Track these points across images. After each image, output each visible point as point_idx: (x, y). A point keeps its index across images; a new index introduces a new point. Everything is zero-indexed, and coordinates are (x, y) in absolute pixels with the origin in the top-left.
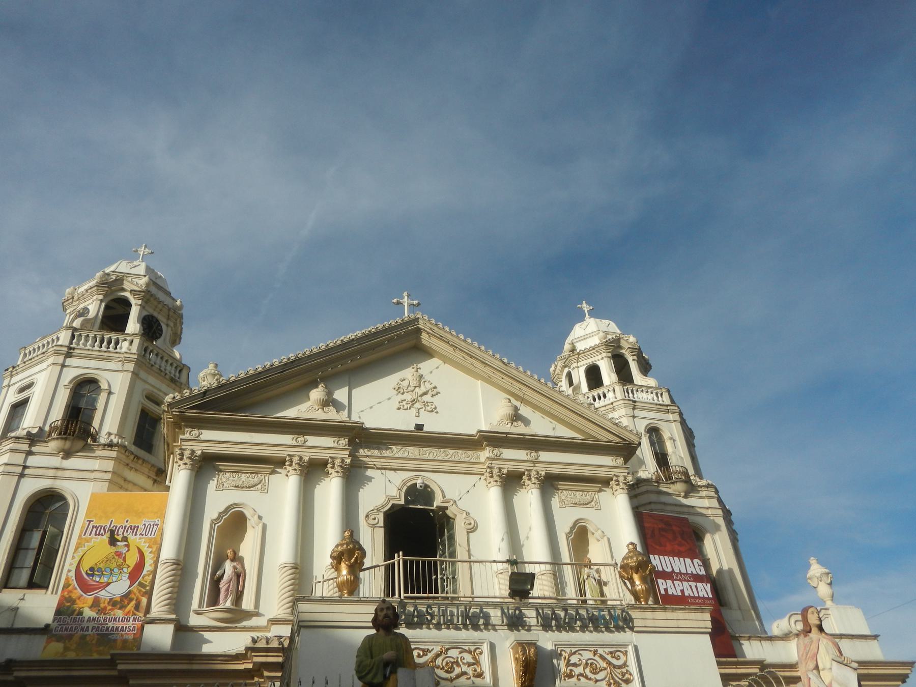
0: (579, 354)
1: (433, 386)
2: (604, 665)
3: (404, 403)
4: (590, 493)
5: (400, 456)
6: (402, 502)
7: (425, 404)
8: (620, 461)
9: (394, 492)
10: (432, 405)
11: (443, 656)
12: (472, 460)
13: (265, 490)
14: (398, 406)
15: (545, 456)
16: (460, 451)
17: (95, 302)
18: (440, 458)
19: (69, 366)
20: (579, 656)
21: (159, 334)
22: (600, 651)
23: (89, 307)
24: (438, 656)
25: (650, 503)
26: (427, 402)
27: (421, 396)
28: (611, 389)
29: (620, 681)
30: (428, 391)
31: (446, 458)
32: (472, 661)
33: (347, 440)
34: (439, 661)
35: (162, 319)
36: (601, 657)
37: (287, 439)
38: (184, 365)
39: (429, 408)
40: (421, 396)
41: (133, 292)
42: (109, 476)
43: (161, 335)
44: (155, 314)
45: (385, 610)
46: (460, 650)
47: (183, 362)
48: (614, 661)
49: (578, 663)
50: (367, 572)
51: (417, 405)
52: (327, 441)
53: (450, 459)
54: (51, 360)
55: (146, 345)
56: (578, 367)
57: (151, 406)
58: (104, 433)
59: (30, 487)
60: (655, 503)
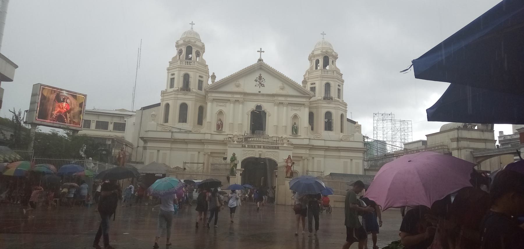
0: (314, 56)
7: (262, 84)
8: (308, 100)
9: (253, 108)
12: (272, 100)
13: (226, 107)
22: (273, 153)
34: (248, 153)
35: (199, 50)
38: (207, 65)
39: (262, 86)
42: (194, 100)
44: (198, 50)
48: (275, 154)
51: (260, 85)
57: (201, 79)
58: (191, 88)
59: (180, 102)
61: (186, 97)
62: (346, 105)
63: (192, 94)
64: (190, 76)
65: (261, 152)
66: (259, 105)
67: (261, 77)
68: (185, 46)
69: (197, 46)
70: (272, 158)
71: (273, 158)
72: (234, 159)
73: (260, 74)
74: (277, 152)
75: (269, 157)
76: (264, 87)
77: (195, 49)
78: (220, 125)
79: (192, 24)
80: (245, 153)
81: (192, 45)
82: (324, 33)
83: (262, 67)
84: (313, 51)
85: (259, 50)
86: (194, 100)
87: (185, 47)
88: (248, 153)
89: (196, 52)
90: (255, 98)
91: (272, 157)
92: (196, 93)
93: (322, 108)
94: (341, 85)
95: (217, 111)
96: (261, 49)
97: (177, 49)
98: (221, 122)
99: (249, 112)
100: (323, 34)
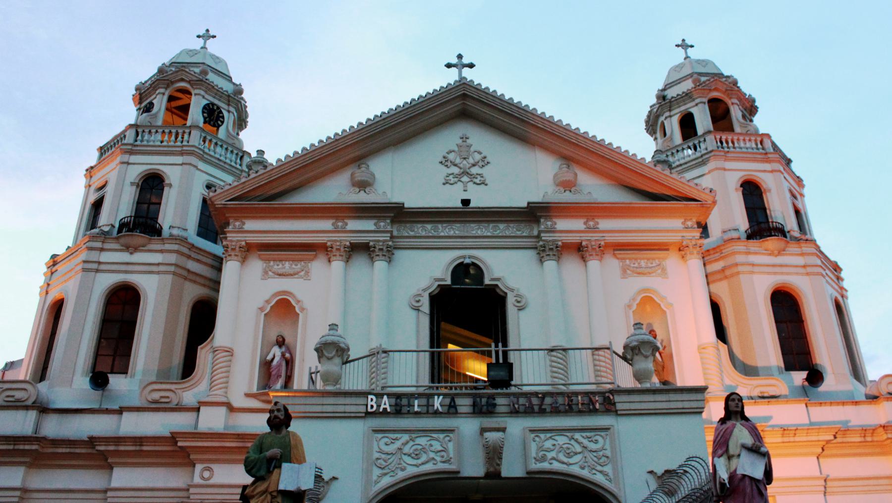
0: (670, 102)
1: (482, 155)
2: (578, 449)
3: (451, 177)
4: (657, 260)
5: (446, 235)
6: (449, 282)
10: (482, 177)
11: (411, 443)
12: (524, 234)
14: (444, 181)
15: (605, 224)
16: (512, 225)
17: (158, 96)
18: (489, 234)
19: (134, 164)
20: (555, 442)
21: (221, 121)
22: (577, 436)
23: (154, 101)
24: (405, 444)
25: (736, 265)
26: (477, 174)
27: (469, 169)
28: (702, 139)
29: (596, 464)
30: (478, 162)
31: (496, 233)
32: (440, 448)
33: (388, 221)
34: (406, 449)
36: (576, 441)
37: (326, 224)
38: (244, 152)
39: (477, 181)
40: (469, 169)
41: (192, 82)
42: (172, 269)
43: (223, 122)
44: (216, 102)
45: (276, 412)
46: (429, 438)
47: (244, 149)
48: (592, 446)
49: (552, 448)
50: (352, 363)
51: (465, 179)
52: (368, 225)
53: (500, 235)
54: (119, 159)
55: (203, 135)
56: (670, 116)
60: (743, 264)
61: (139, 257)
62: (836, 268)
63: (167, 247)
64: (167, 182)
65: (499, 435)
66: (467, 261)
67: (470, 146)
68: (166, 89)
69: (210, 88)
70: (575, 470)
71: (585, 473)
72: (275, 451)
73: (464, 138)
74: (607, 429)
75: (556, 466)
76: (483, 185)
77: (204, 97)
78: (279, 365)
79: (207, 36)
80: (392, 448)
81: (189, 82)
82: (686, 42)
83: (469, 103)
84: (664, 90)
85: (454, 61)
86: (172, 269)
87: (162, 90)
88: (406, 449)
89: (204, 108)
90: (444, 230)
91: (576, 468)
92: (183, 240)
93: (752, 273)
94: (798, 196)
95: (267, 297)
96: (460, 57)
97: (138, 107)
98: (289, 350)
99: (420, 295)
100: (684, 45)
